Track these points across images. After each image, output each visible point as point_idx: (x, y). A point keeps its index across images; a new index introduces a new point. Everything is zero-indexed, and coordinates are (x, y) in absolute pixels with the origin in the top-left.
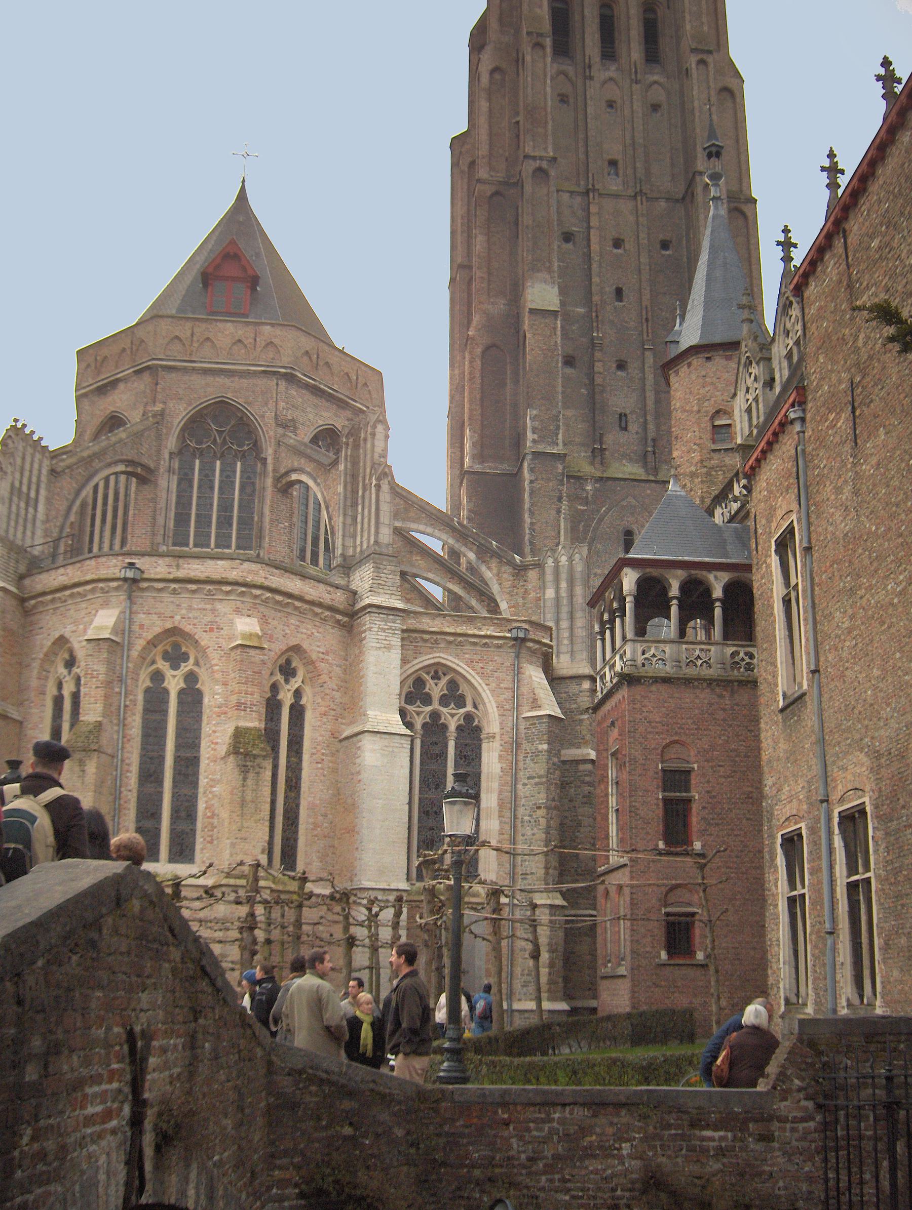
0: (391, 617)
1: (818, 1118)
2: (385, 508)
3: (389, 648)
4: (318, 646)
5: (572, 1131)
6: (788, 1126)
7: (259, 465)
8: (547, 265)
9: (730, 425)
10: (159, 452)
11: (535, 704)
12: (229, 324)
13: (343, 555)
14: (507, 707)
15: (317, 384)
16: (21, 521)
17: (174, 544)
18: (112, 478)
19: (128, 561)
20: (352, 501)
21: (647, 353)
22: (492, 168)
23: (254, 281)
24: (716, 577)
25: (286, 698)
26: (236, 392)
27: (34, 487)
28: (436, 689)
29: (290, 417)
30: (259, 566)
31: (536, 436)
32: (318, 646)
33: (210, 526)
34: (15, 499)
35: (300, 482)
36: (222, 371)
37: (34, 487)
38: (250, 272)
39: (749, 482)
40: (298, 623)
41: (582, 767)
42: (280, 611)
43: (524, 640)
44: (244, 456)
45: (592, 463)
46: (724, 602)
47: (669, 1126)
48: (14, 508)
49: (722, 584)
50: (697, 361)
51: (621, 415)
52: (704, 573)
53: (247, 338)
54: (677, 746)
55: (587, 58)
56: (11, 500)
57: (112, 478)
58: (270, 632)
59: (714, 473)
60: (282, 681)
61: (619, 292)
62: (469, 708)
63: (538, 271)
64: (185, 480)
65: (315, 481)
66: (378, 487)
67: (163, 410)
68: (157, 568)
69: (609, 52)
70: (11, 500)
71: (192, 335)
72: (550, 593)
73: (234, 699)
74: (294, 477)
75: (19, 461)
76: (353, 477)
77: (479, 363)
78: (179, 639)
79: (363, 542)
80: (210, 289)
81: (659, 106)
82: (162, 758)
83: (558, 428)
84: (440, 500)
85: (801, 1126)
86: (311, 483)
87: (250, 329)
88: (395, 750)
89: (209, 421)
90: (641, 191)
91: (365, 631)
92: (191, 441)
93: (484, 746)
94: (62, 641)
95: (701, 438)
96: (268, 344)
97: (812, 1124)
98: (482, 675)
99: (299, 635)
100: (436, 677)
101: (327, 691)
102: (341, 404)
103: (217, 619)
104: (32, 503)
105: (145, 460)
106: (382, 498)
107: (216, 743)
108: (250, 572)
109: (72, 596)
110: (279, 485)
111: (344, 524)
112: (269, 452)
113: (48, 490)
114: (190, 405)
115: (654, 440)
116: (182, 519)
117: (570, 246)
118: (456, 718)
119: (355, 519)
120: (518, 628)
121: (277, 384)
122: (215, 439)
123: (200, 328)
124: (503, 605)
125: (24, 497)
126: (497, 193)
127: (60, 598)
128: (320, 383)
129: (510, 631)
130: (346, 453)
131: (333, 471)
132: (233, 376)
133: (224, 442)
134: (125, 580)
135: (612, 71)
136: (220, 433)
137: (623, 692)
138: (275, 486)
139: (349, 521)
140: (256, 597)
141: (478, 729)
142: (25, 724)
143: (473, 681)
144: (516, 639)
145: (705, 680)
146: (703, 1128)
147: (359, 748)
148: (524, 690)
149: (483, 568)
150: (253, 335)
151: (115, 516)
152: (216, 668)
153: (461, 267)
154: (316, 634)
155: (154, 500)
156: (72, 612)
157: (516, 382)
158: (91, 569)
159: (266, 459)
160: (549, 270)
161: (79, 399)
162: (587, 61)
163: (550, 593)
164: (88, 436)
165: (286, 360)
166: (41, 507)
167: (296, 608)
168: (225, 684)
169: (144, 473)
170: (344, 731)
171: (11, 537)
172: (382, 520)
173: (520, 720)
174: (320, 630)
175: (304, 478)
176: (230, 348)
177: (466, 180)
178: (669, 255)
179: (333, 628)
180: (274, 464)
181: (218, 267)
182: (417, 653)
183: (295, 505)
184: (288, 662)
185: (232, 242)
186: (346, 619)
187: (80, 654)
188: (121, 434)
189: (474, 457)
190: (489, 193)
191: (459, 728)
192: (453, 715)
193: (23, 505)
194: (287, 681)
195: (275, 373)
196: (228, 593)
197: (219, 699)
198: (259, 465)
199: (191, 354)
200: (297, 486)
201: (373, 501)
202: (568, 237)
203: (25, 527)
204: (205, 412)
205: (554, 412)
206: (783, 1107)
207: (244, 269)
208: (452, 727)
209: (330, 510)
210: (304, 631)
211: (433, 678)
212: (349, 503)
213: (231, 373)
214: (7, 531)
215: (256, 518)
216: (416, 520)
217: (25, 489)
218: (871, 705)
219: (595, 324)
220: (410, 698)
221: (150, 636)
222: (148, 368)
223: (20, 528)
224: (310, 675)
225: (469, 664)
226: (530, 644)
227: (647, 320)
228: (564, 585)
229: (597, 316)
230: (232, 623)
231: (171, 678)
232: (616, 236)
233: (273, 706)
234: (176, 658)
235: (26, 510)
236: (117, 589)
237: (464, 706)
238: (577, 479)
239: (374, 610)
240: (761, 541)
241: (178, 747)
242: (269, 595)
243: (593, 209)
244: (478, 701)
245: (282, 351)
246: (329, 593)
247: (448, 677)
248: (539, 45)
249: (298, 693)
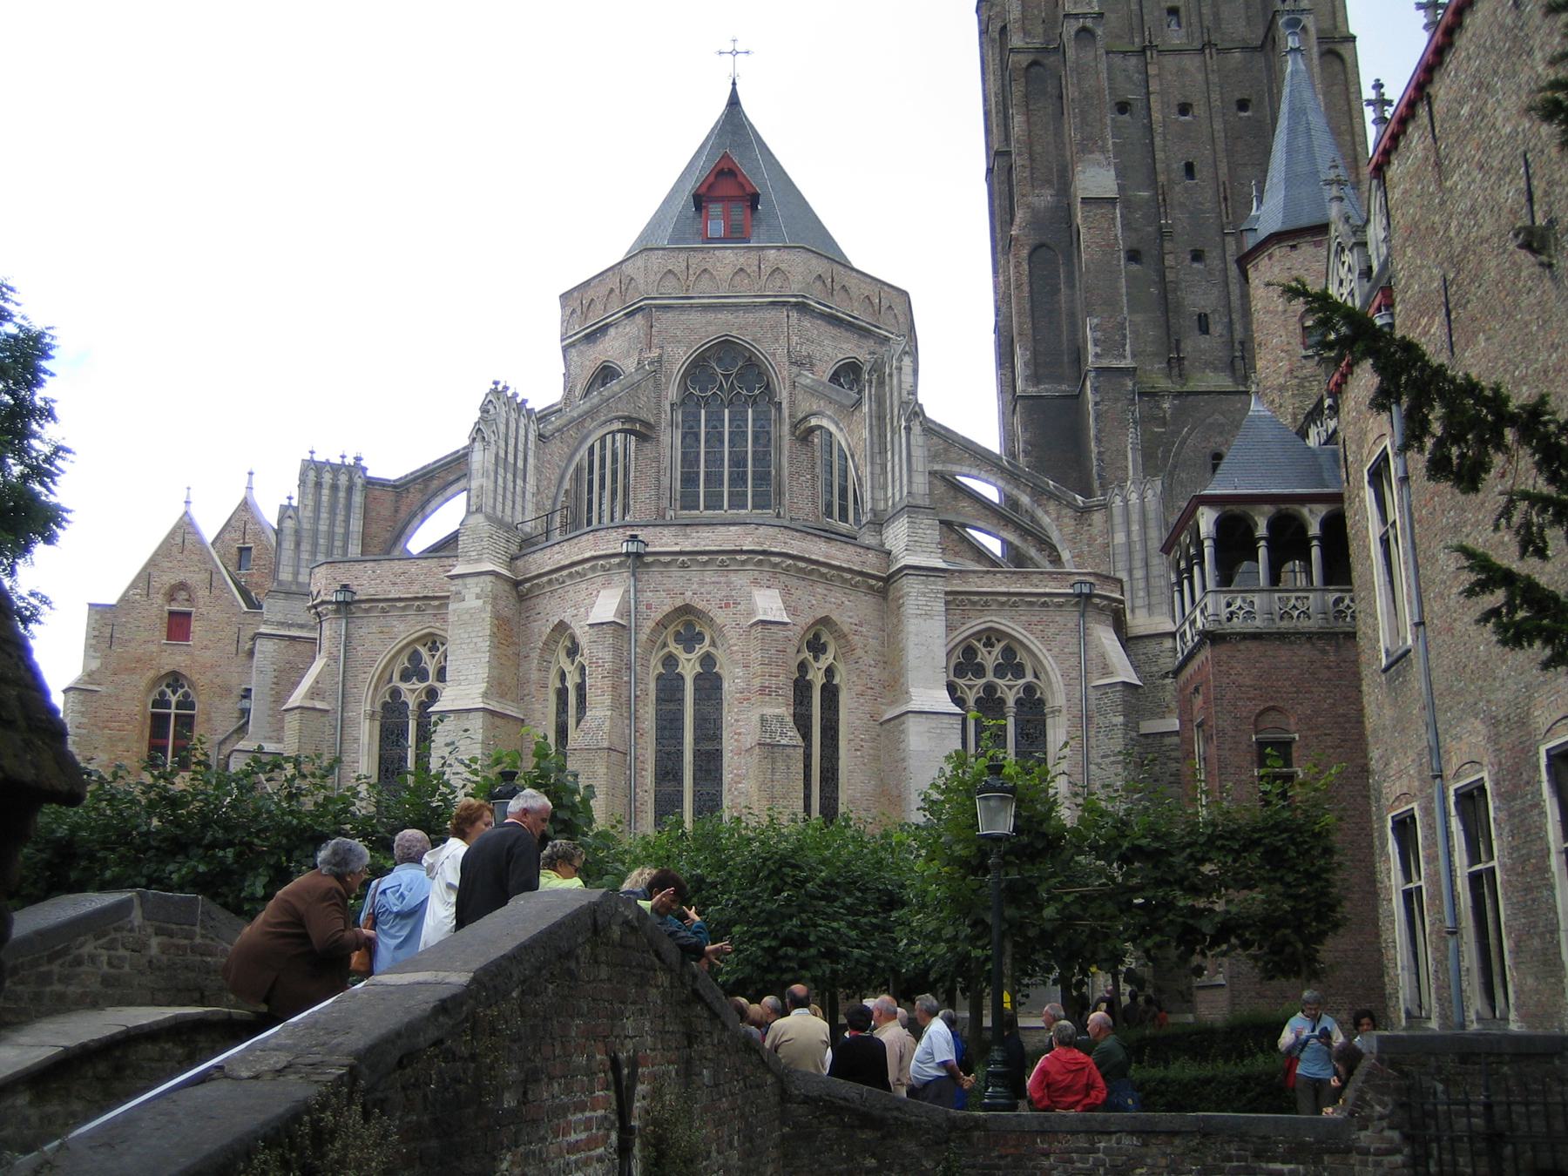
1: (1406, 1150)
2: (918, 453)
3: (928, 615)
5: (1119, 1163)
6: (1371, 1159)
8: (1100, 143)
10: (658, 404)
11: (1106, 670)
14: (1074, 674)
16: (509, 495)
17: (683, 508)
18: (609, 438)
19: (629, 533)
20: (880, 448)
21: (1229, 239)
22: (1026, 33)
23: (753, 200)
24: (1311, 511)
25: (817, 678)
27: (521, 456)
28: (990, 658)
30: (777, 529)
31: (1098, 350)
33: (722, 484)
34: (501, 471)
35: (820, 427)
36: (724, 306)
37: (521, 456)
38: (748, 189)
41: (1167, 741)
42: (804, 579)
43: (1090, 596)
44: (755, 402)
45: (1169, 376)
47: (1229, 1158)
48: (500, 481)
49: (1319, 519)
50: (1278, 251)
51: (1200, 316)
52: (1296, 507)
53: (750, 266)
54: (1273, 713)
56: (496, 472)
57: (609, 438)
59: (1307, 384)
60: (811, 659)
61: (1189, 169)
62: (1029, 678)
63: (1092, 152)
64: (690, 435)
65: (837, 425)
66: (908, 429)
67: (661, 356)
68: (664, 541)
70: (496, 472)
72: (1120, 538)
73: (757, 682)
74: (814, 422)
75: (502, 428)
76: (880, 418)
77: (1026, 267)
78: (692, 618)
79: (896, 493)
82: (680, 753)
83: (1124, 336)
84: (988, 435)
85: (1387, 1160)
86: (833, 428)
87: (754, 255)
88: (946, 731)
90: (1209, 42)
91: (902, 597)
93: (1049, 721)
94: (562, 627)
95: (1289, 343)
97: (1398, 1159)
98: (1043, 639)
99: (827, 605)
100: (989, 644)
101: (864, 668)
102: (864, 332)
103: (733, 593)
104: (520, 473)
105: (644, 415)
106: (913, 441)
107: (740, 734)
109: (570, 575)
112: (784, 395)
113: (537, 458)
114: (689, 348)
115: (1242, 343)
116: (689, 480)
117: (1126, 117)
118: (1015, 689)
120: (1081, 582)
123: (696, 259)
124: (1066, 556)
125: (511, 469)
126: (1034, 63)
127: (557, 580)
129: (1072, 586)
131: (857, 413)
132: (737, 311)
133: (732, 387)
134: (628, 554)
136: (727, 377)
137: (1206, 653)
138: (793, 434)
139: (878, 469)
140: (776, 565)
141: (1041, 702)
142: (527, 721)
143: (1032, 646)
144: (1079, 595)
145: (1303, 634)
146: (1270, 1160)
147: (902, 732)
148: (1092, 654)
149: (1039, 513)
151: (614, 480)
152: (735, 648)
153: (998, 154)
155: (657, 460)
156: (571, 593)
157: (1071, 286)
158: (585, 547)
160: (1103, 150)
161: (565, 349)
163: (1120, 538)
164: (578, 391)
165: (795, 288)
166: (531, 480)
167: (822, 575)
168: (746, 666)
169: (643, 430)
170: (885, 711)
171: (499, 514)
172: (914, 467)
173: (1090, 690)
175: (825, 423)
177: (998, 50)
178: (1249, 117)
179: (866, 594)
180: (790, 408)
181: (711, 186)
182: (965, 618)
183: (818, 454)
184: (817, 636)
185: (725, 157)
187: (583, 641)
188: (614, 386)
189: (1027, 379)
190: (1024, 65)
191: (1019, 702)
192: (1010, 688)
193: (510, 477)
194: (816, 658)
195: (785, 304)
196: (744, 562)
197: (741, 684)
200: (818, 432)
202: (1123, 107)
203: (514, 502)
205: (1119, 319)
206: (1365, 1137)
207: (742, 186)
208: (1011, 702)
211: (985, 645)
213: (736, 307)
214: (494, 508)
215: (773, 473)
216: (959, 462)
217: (511, 459)
218: (1485, 662)
219: (1162, 210)
220: (960, 670)
221: (659, 616)
222: (640, 309)
223: (509, 503)
224: (844, 650)
225: (1028, 626)
226: (1097, 601)
227: (1225, 199)
228: (1135, 528)
229: (1164, 200)
230: (750, 596)
231: (685, 662)
232: (1183, 100)
233: (802, 688)
234: (690, 639)
235: (514, 482)
236: (620, 565)
237: (1024, 676)
238: (1152, 395)
240: (1351, 471)
241: (697, 740)
243: (1152, 70)
244: (1039, 669)
245: (791, 278)
246: (859, 555)
247: (1002, 644)
249: (830, 672)
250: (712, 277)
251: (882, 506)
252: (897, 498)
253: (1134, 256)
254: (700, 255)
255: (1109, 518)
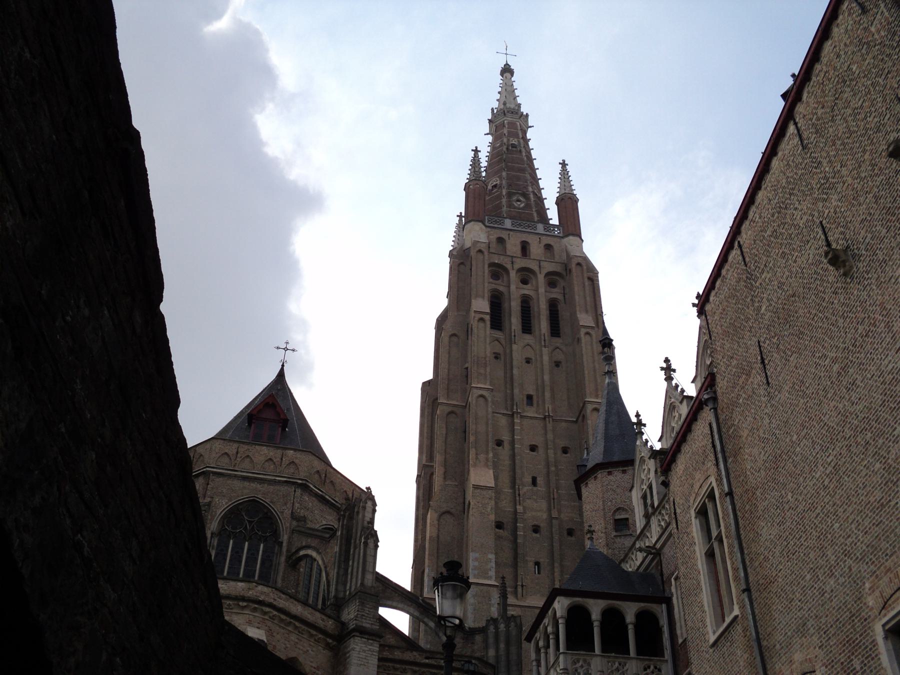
0: (371, 642)
4: (311, 662)
7: (277, 547)
9: (627, 519)
12: (265, 447)
13: (336, 597)
15: (324, 495)
23: (284, 423)
26: (264, 494)
29: (302, 515)
30: (270, 589)
32: (311, 662)
36: (256, 479)
38: (282, 416)
39: (666, 478)
40: (296, 640)
42: (284, 628)
46: (637, 627)
50: (601, 474)
53: (276, 458)
55: (513, 330)
58: (274, 643)
61: (534, 482)
65: (319, 553)
66: (366, 544)
67: (210, 502)
69: (527, 328)
71: (237, 453)
74: (302, 553)
80: (253, 426)
81: (560, 362)
86: (314, 554)
87: (279, 452)
89: (244, 514)
91: (349, 652)
92: (228, 527)
96: (290, 463)
106: (368, 552)
108: (262, 593)
110: (290, 561)
111: (338, 573)
112: (285, 538)
119: (347, 570)
121: (295, 491)
122: (246, 526)
123: (243, 448)
128: (326, 495)
130: (343, 522)
131: (332, 541)
132: (264, 483)
135: (528, 338)
138: (287, 561)
139: (342, 572)
140: (265, 613)
150: (280, 457)
154: (310, 651)
159: (282, 543)
162: (513, 334)
165: (302, 475)
167: (296, 628)
174: (314, 649)
176: (263, 464)
180: (288, 546)
186: (335, 643)
196: (243, 608)
198: (277, 547)
199: (234, 466)
201: (362, 554)
204: (241, 507)
209: (328, 569)
210: (301, 648)
212: (343, 560)
213: (262, 481)
228: (502, 646)
239: (358, 634)
242: (275, 613)
246: (323, 620)
248: (482, 320)
250: (252, 461)
251: (341, 595)
252: (353, 589)
253: (499, 525)
254: (246, 447)
255: (486, 641)
